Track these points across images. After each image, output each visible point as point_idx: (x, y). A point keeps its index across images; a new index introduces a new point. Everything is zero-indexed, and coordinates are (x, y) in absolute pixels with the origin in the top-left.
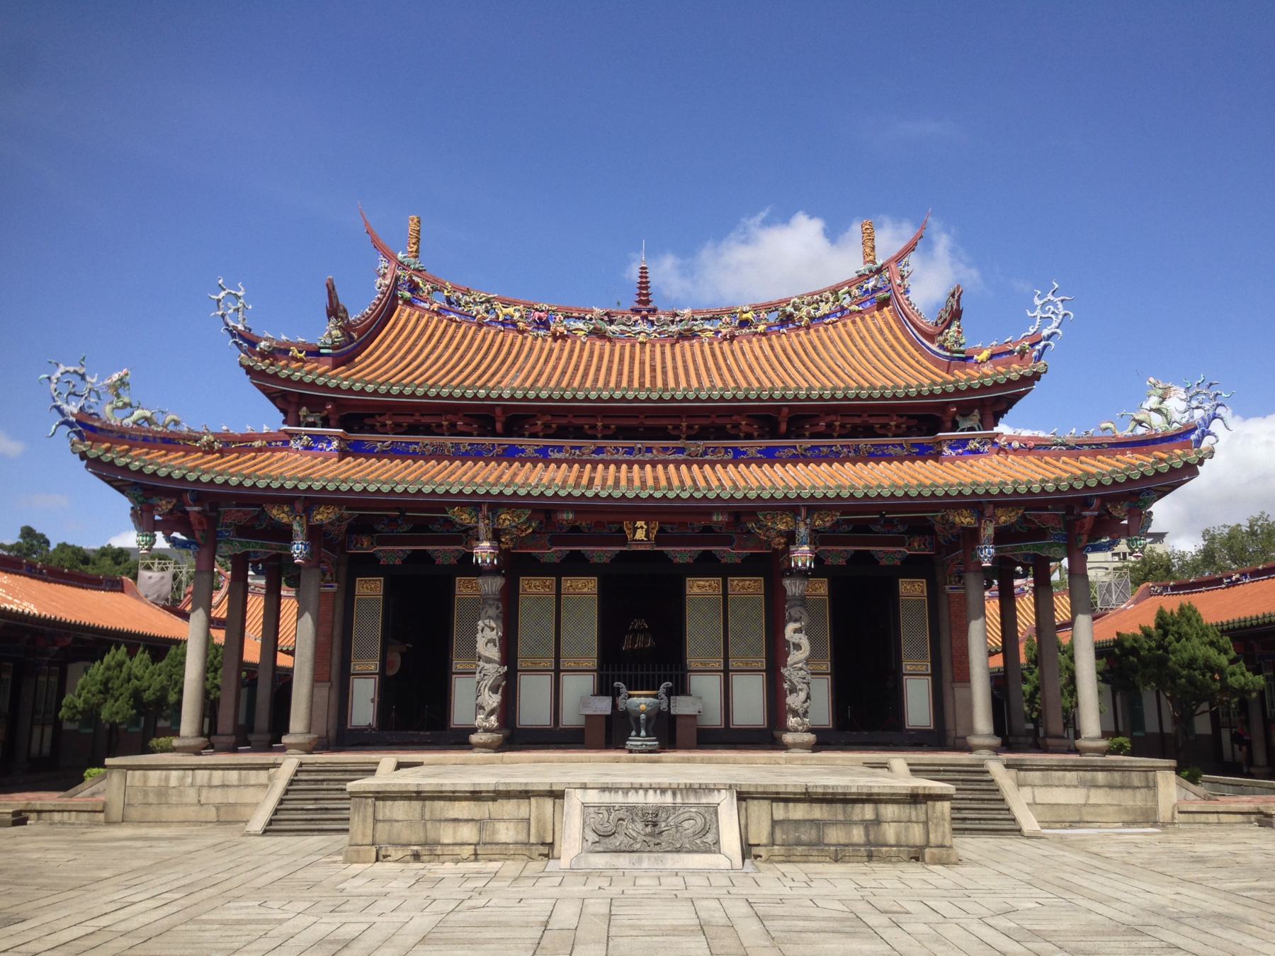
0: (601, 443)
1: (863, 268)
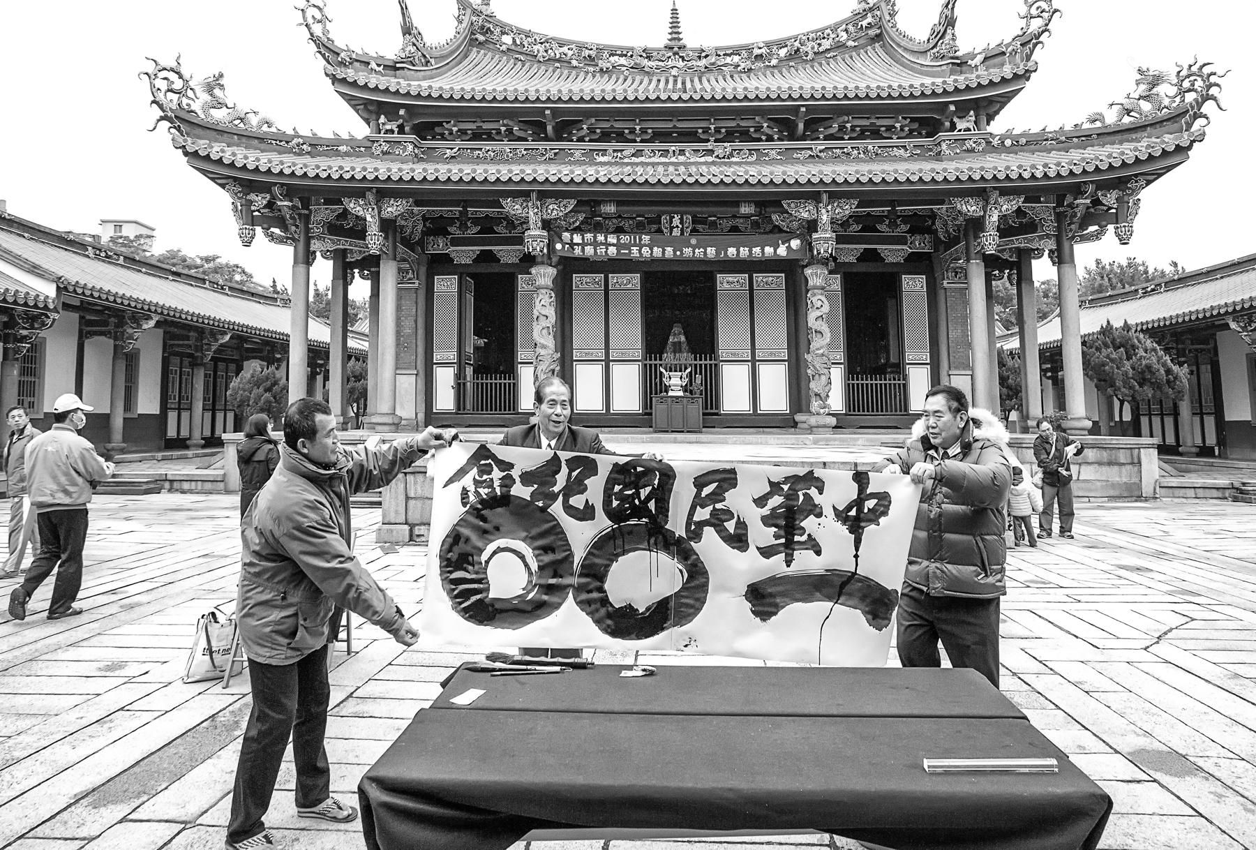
0: (640, 146)
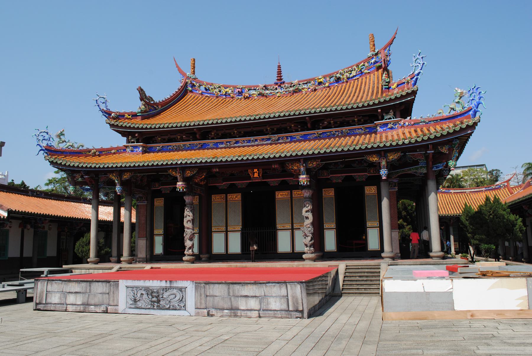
1: (370, 54)
